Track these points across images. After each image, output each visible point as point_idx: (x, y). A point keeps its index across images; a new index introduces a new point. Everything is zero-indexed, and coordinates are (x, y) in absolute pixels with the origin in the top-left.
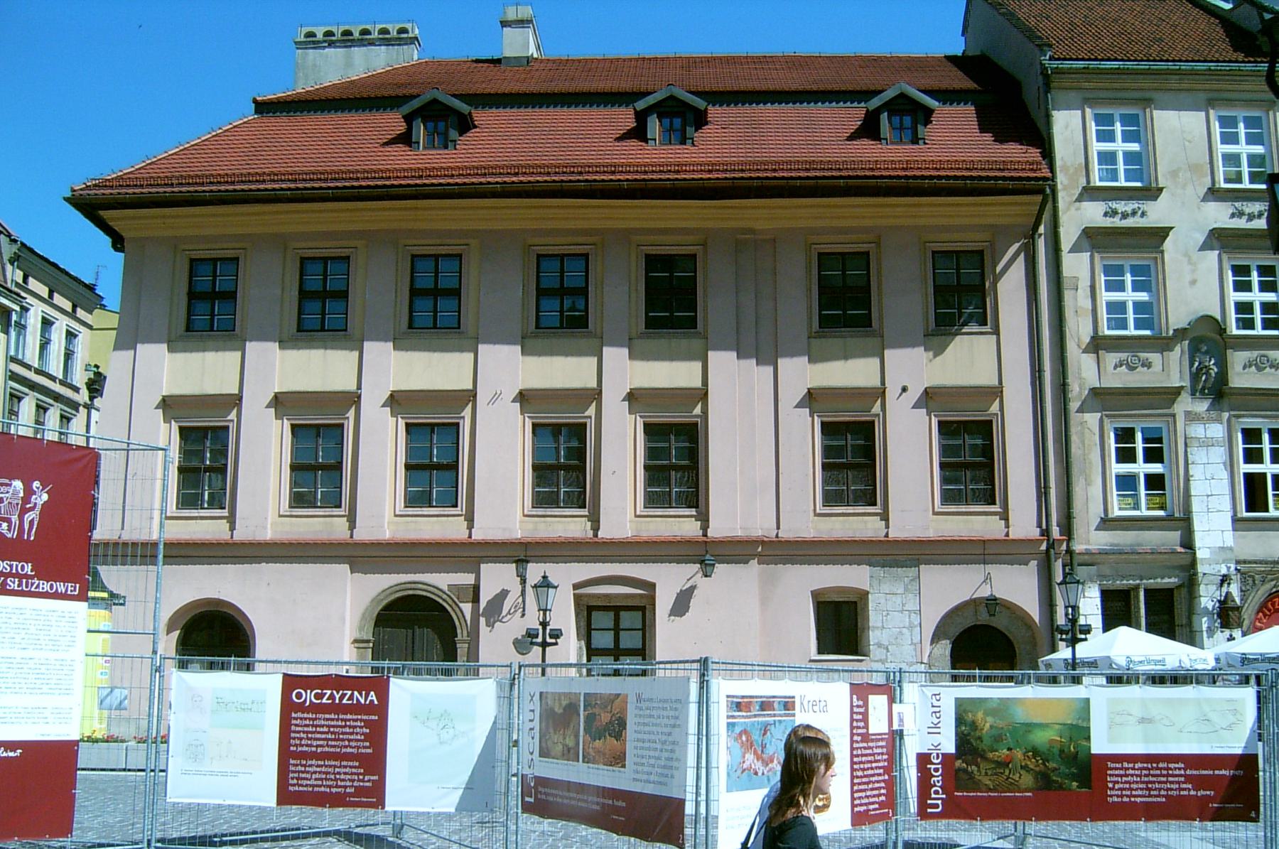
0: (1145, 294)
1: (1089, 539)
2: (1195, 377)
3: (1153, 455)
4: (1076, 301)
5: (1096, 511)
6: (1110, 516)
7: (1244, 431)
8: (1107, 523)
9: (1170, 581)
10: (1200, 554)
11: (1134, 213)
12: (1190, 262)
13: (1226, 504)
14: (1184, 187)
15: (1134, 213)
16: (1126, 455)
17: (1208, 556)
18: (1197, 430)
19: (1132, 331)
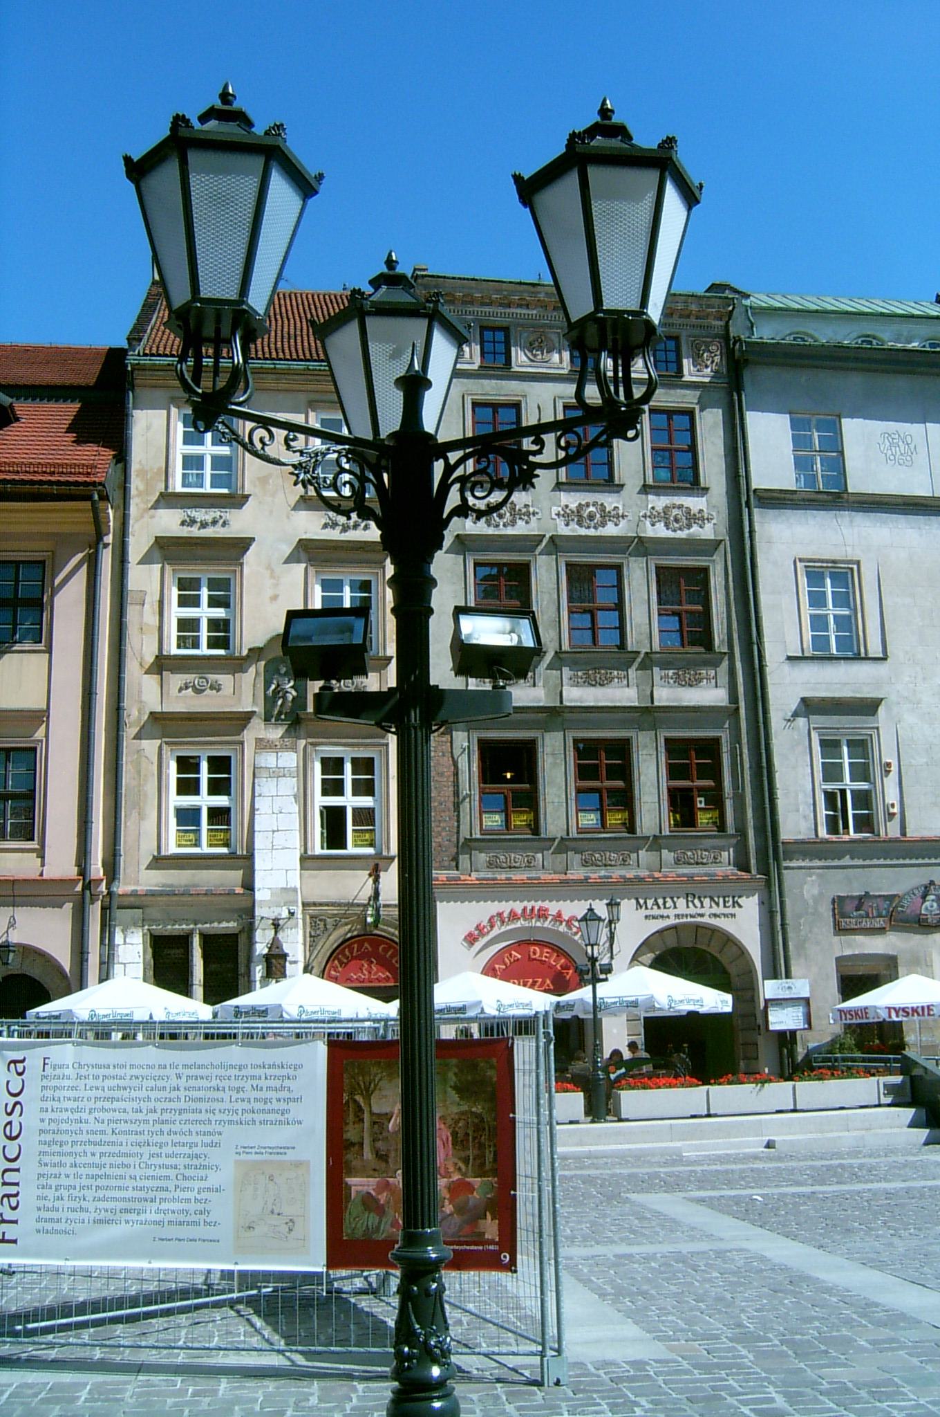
0: (222, 610)
1: (138, 878)
2: (270, 701)
3: (217, 787)
4: (140, 618)
5: (148, 848)
6: (163, 853)
7: (324, 761)
8: (160, 861)
9: (230, 926)
10: (259, 896)
11: (214, 522)
12: (272, 576)
13: (296, 840)
14: (273, 495)
15: (214, 522)
16: (188, 787)
17: (268, 898)
18: (269, 760)
19: (204, 650)
